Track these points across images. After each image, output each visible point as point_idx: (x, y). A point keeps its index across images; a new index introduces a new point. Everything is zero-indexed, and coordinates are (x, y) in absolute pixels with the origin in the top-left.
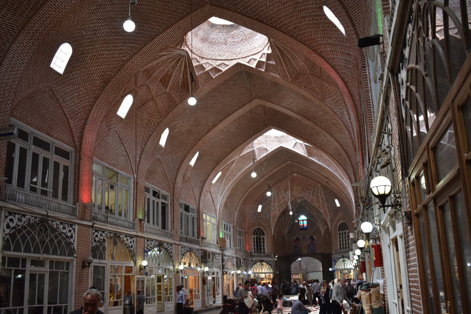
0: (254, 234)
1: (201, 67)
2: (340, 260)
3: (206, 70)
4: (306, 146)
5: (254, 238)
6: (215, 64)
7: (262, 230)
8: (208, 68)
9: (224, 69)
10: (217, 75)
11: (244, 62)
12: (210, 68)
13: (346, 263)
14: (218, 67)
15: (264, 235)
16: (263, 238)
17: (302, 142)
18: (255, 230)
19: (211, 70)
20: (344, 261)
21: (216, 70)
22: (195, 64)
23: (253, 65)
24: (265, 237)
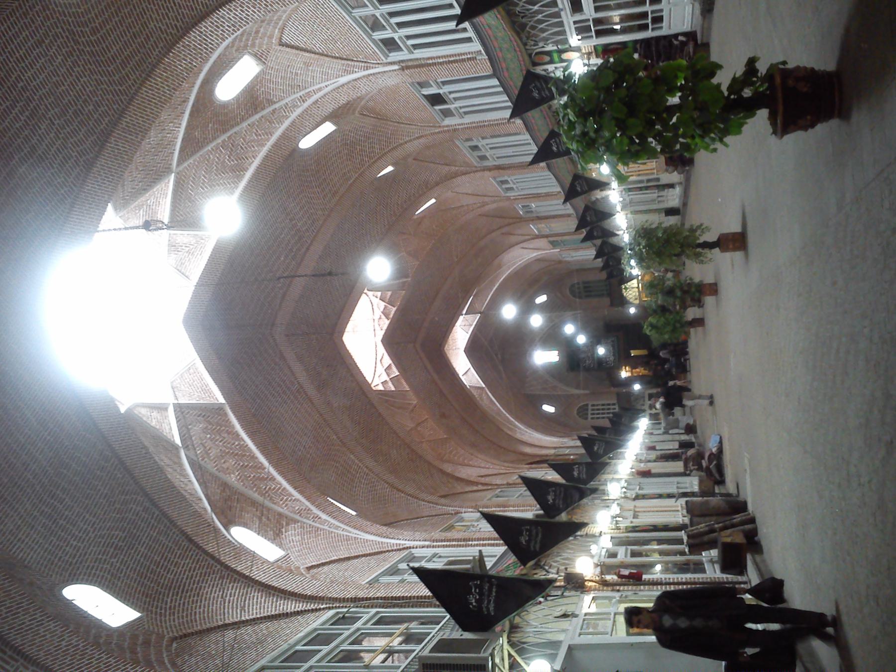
0: (586, 419)
3: (388, 379)
4: (465, 314)
5: (592, 418)
6: (381, 370)
7: (580, 407)
8: (385, 377)
9: (387, 361)
10: (394, 368)
11: (381, 334)
12: (384, 373)
14: (385, 367)
15: (587, 405)
16: (593, 405)
17: (461, 318)
18: (580, 417)
19: (388, 375)
22: (381, 388)
23: (386, 323)
24: (590, 403)
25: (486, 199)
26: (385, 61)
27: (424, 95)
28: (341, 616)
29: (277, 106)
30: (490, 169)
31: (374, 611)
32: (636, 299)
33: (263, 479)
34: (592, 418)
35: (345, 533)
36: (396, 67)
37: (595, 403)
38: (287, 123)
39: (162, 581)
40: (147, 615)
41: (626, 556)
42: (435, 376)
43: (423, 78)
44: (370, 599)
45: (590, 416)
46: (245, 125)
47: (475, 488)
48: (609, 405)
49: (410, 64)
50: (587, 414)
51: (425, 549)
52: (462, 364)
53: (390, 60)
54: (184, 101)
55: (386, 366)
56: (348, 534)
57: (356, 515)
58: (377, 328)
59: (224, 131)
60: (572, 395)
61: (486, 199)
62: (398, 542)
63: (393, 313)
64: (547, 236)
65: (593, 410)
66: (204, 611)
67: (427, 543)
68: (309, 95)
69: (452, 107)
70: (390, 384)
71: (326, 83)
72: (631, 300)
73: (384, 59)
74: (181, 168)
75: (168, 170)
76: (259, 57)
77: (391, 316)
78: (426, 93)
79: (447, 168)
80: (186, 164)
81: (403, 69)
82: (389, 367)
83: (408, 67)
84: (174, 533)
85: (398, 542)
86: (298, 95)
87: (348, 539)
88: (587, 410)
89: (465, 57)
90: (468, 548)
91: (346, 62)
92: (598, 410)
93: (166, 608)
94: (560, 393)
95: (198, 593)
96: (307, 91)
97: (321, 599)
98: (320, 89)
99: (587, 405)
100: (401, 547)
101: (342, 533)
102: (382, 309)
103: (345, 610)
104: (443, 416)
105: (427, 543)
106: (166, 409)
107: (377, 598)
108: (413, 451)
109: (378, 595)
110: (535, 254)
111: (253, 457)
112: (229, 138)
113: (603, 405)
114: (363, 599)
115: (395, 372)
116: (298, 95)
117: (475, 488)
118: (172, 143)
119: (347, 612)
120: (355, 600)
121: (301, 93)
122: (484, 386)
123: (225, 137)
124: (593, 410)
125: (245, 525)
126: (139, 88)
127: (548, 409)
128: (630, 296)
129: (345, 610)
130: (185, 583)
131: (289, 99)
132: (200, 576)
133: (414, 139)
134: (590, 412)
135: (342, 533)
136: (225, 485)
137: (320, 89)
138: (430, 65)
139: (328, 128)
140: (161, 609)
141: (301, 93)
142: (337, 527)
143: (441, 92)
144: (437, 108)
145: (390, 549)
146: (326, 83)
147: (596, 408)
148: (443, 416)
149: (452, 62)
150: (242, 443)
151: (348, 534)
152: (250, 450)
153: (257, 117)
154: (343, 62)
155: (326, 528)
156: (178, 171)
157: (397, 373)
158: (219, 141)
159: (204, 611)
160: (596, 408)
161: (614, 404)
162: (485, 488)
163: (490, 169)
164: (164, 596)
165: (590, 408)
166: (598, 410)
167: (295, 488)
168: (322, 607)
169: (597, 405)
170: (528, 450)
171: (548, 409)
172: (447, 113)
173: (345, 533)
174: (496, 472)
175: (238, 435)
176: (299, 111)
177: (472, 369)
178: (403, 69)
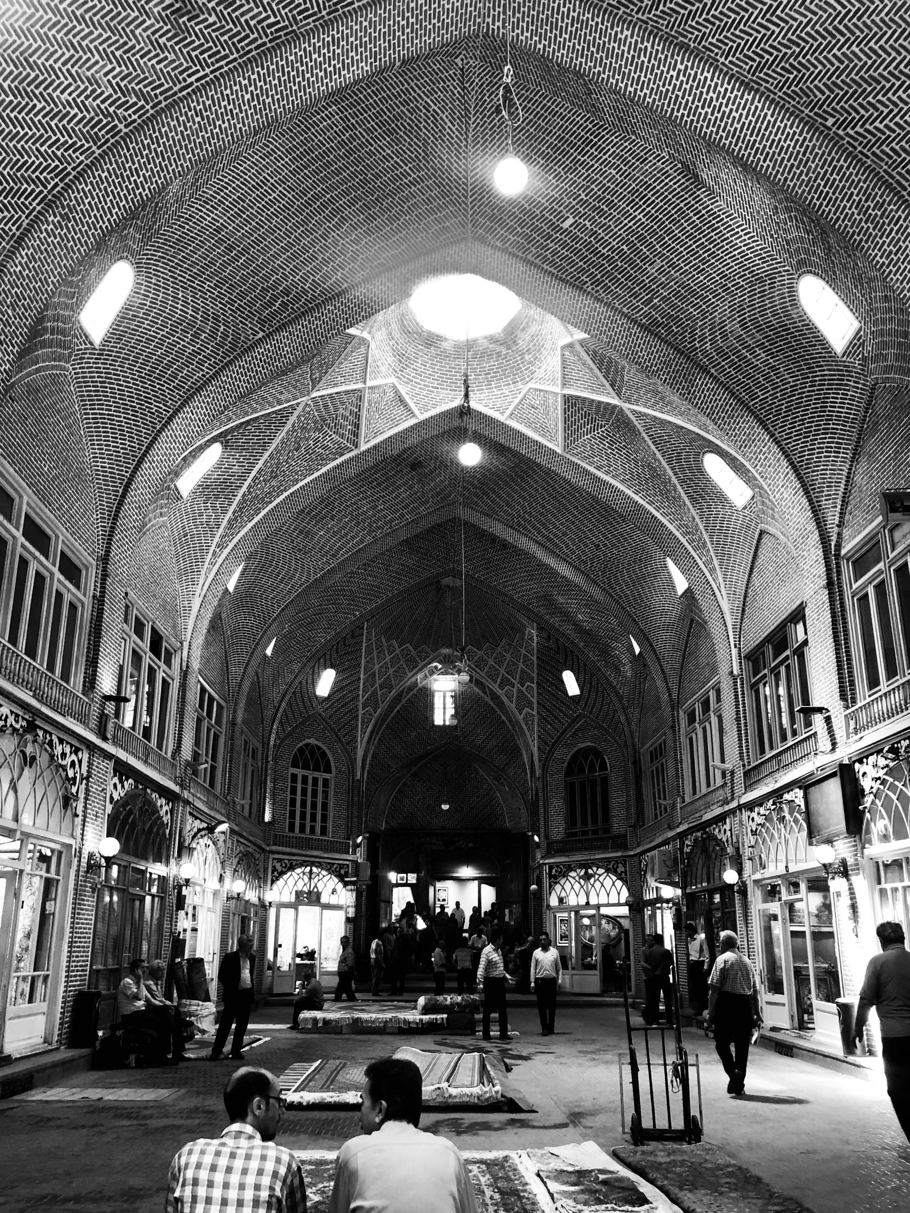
0: (295, 765)
2: (573, 874)
5: (294, 777)
7: (324, 754)
13: (598, 885)
15: (328, 770)
16: (326, 782)
18: (300, 749)
20: (587, 877)
32: (561, 900)
37: (332, 785)
45: (300, 772)
48: (324, 819)
50: (306, 767)
65: (315, 781)
72: (558, 888)
88: (317, 769)
92: (315, 794)
94: (361, 712)
99: (328, 770)
113: (325, 806)
122: (364, 447)
124: (315, 781)
128: (567, 886)
134: (311, 774)
147: (320, 788)
160: (320, 788)
161: (324, 831)
166: (315, 794)
169: (325, 793)
177: (412, 422)
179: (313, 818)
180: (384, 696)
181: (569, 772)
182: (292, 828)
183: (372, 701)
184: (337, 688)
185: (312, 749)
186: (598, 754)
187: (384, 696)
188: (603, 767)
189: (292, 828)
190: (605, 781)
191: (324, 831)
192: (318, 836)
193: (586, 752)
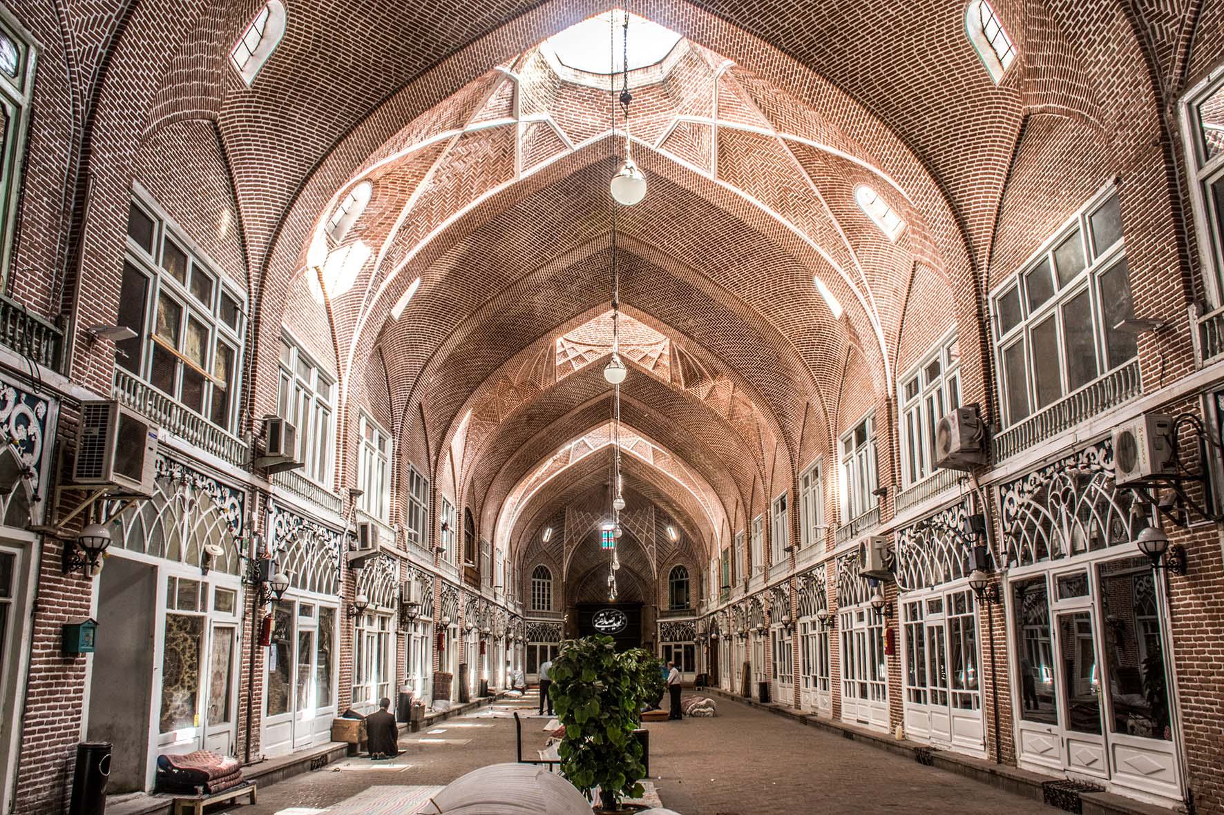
0: (534, 577)
1: (565, 354)
3: (569, 358)
5: (534, 583)
6: (581, 350)
7: (547, 570)
8: (572, 354)
10: (582, 365)
12: (577, 354)
16: (549, 584)
19: (574, 359)
21: (580, 358)
25: (768, 481)
26: (897, 380)
27: (864, 423)
28: (239, 305)
29: (852, 253)
30: (795, 488)
31: (242, 343)
33: (429, 218)
34: (534, 583)
35: (362, 309)
36: (890, 393)
38: (835, 264)
39: (292, 108)
40: (249, 92)
41: (300, 626)
42: (576, 411)
43: (879, 423)
44: (256, 338)
45: (537, 580)
46: (831, 216)
47: (432, 452)
49: (893, 408)
50: (539, 577)
51: (338, 398)
52: (595, 440)
53: (898, 386)
54: (851, 150)
55: (585, 356)
56: (361, 312)
57: (390, 317)
58: (630, 349)
59: (823, 194)
60: (562, 562)
61: (768, 481)
62: (349, 368)
63: (646, 367)
64: (733, 546)
65: (544, 584)
66: (252, 154)
67: (344, 400)
68: (864, 290)
69: (853, 452)
70: (564, 360)
71: (876, 312)
73: (901, 377)
74: (781, 142)
75: (779, 128)
76: (902, 238)
77: (642, 364)
78: (867, 423)
79: (798, 439)
80: (786, 148)
81: (888, 400)
82: (583, 360)
83: (889, 406)
84: (349, 122)
85: (349, 368)
86: (863, 278)
87: (355, 312)
88: (544, 578)
89: (897, 473)
90: (335, 446)
91: (897, 335)
93: (257, 112)
95: (275, 148)
96: (868, 288)
97: (262, 285)
98: (870, 304)
100: (342, 371)
101: (363, 305)
102: (650, 355)
103: (246, 311)
104: (531, 418)
105: (344, 400)
106: (511, 115)
107: (256, 347)
108: (479, 383)
109: (261, 348)
110: (717, 531)
111: (455, 208)
112: (816, 198)
113: (549, 595)
114: (257, 330)
115: (578, 367)
116: (863, 278)
117: (432, 452)
118: (808, 134)
119: (242, 314)
120: (257, 321)
121: (865, 282)
123: (818, 194)
124: (544, 584)
125: (373, 199)
126: (858, 101)
127: (547, 535)
129: (246, 311)
130: (289, 134)
131: (860, 268)
132: (296, 150)
133: (823, 406)
134: (541, 581)
135: (363, 305)
136: (421, 176)
137: (870, 304)
138: (890, 431)
139: (836, 309)
140: (255, 107)
141: (865, 282)
142: (369, 300)
143: (868, 441)
144: (853, 435)
145: (340, 359)
146: (876, 312)
148: (531, 418)
149: (892, 457)
150: (473, 196)
151: (361, 312)
152: (463, 206)
153: (840, 230)
154: (898, 332)
155: (369, 287)
156: (779, 139)
157: (576, 369)
158: (813, 187)
159: (252, 154)
161: (549, 608)
162: (432, 464)
163: (795, 488)
164: (273, 110)
165: (546, 581)
167: (418, 255)
168: (252, 284)
169: (549, 590)
170: (489, 512)
171: (547, 535)
172: (848, 443)
173: (362, 309)
174: (457, 475)
175: (482, 192)
176: (847, 278)
178: (888, 400)
179: (544, 602)
180: (577, 539)
181: (671, 578)
182: (534, 608)
183: (571, 542)
184: (554, 537)
185: (542, 568)
186: (685, 569)
187: (577, 539)
188: (687, 576)
189: (534, 608)
190: (687, 582)
191: (549, 608)
192: (546, 610)
193: (679, 568)
